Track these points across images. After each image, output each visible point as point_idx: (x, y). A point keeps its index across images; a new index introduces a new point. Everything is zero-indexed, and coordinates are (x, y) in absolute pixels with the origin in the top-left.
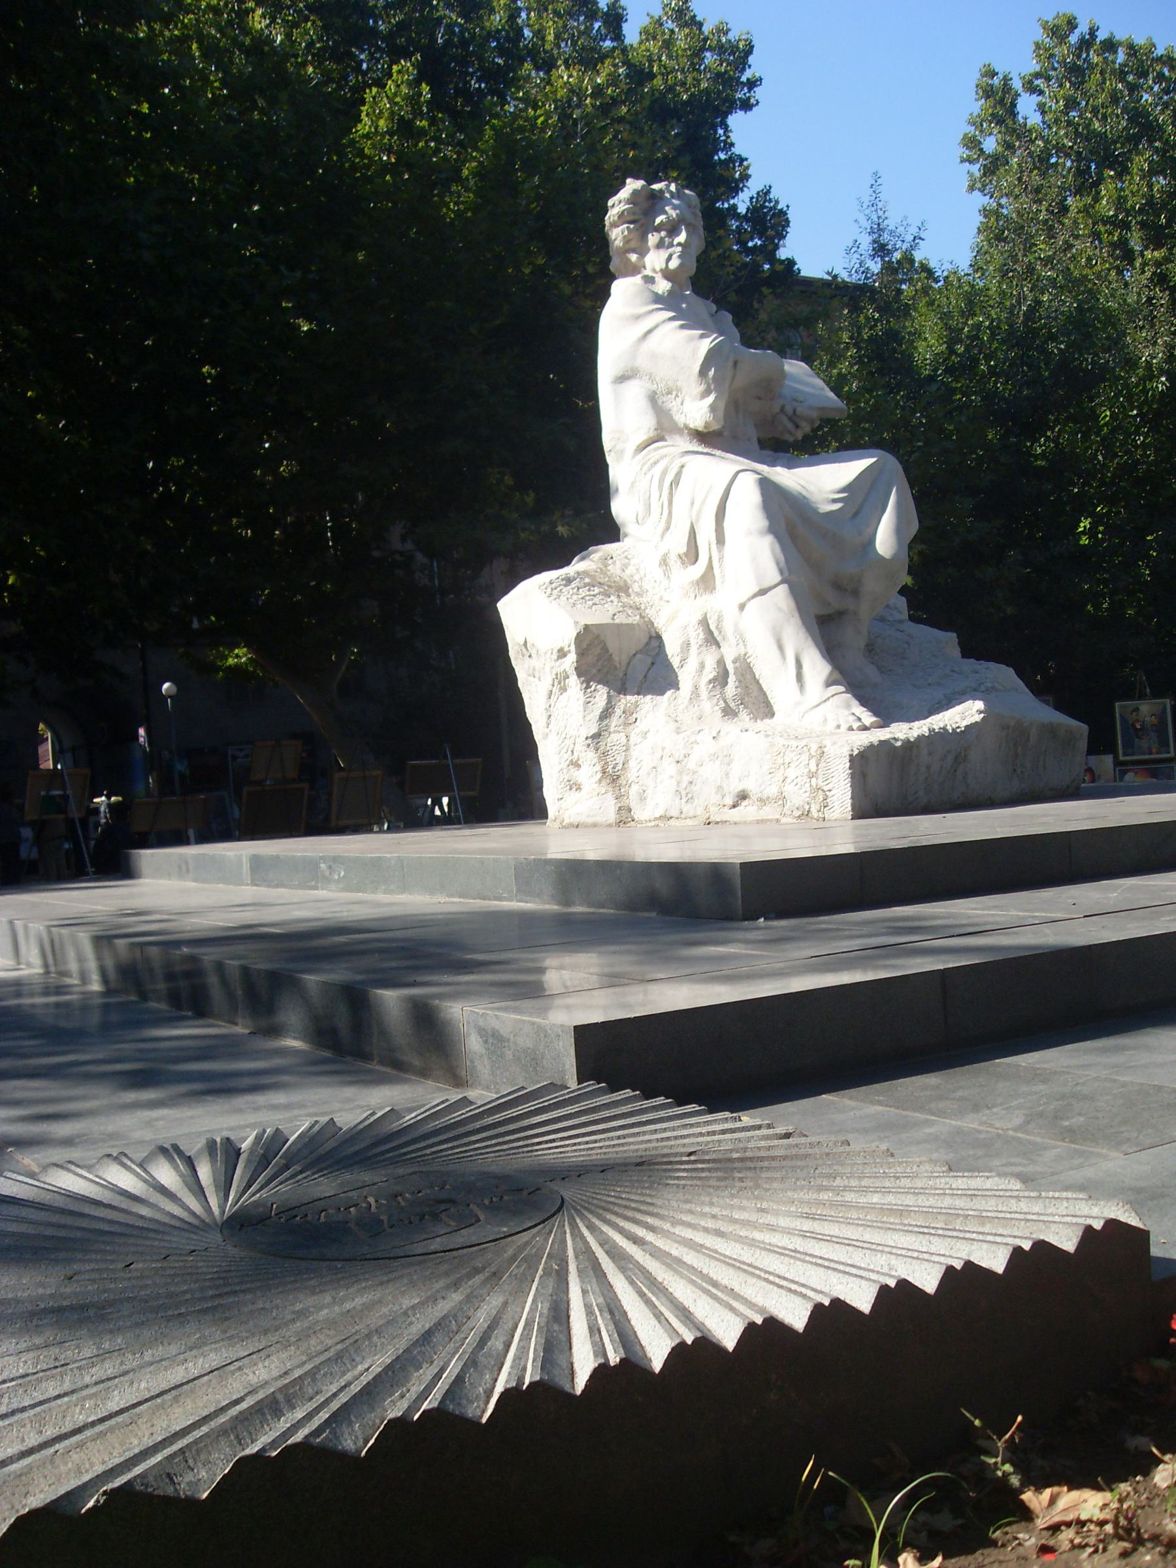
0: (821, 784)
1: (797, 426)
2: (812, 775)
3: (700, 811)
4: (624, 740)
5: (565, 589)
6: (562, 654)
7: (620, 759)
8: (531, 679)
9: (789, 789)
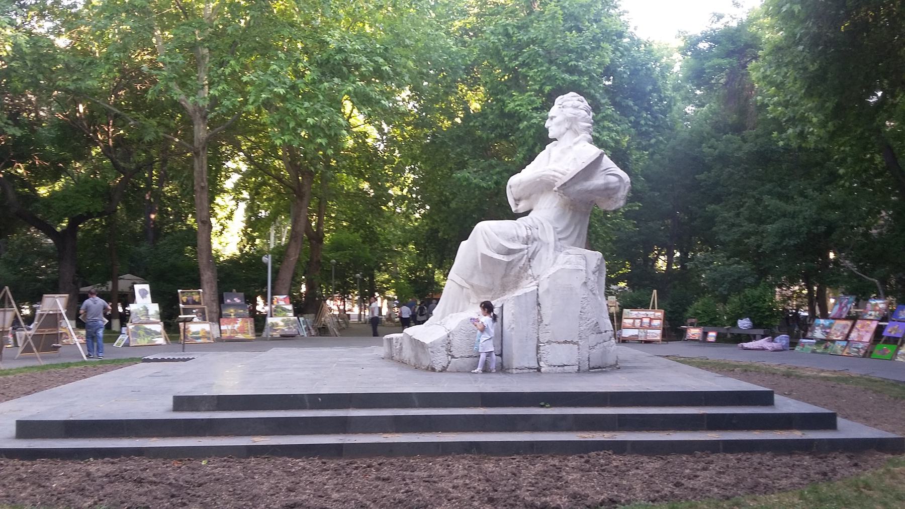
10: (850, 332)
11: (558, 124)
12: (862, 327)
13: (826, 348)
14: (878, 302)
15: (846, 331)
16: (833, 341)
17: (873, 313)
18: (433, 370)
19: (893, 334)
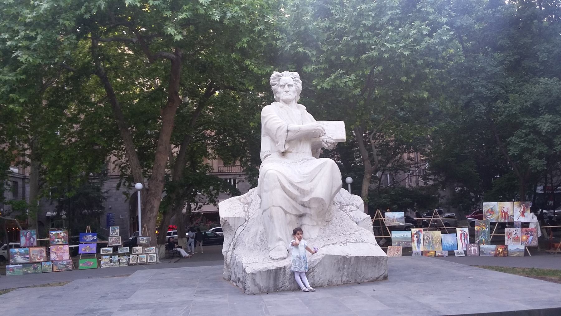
10: (48, 253)
11: (294, 92)
12: (58, 250)
13: (35, 268)
14: (58, 232)
15: (44, 254)
16: (40, 263)
17: (59, 240)
18: (385, 278)
19: (87, 251)
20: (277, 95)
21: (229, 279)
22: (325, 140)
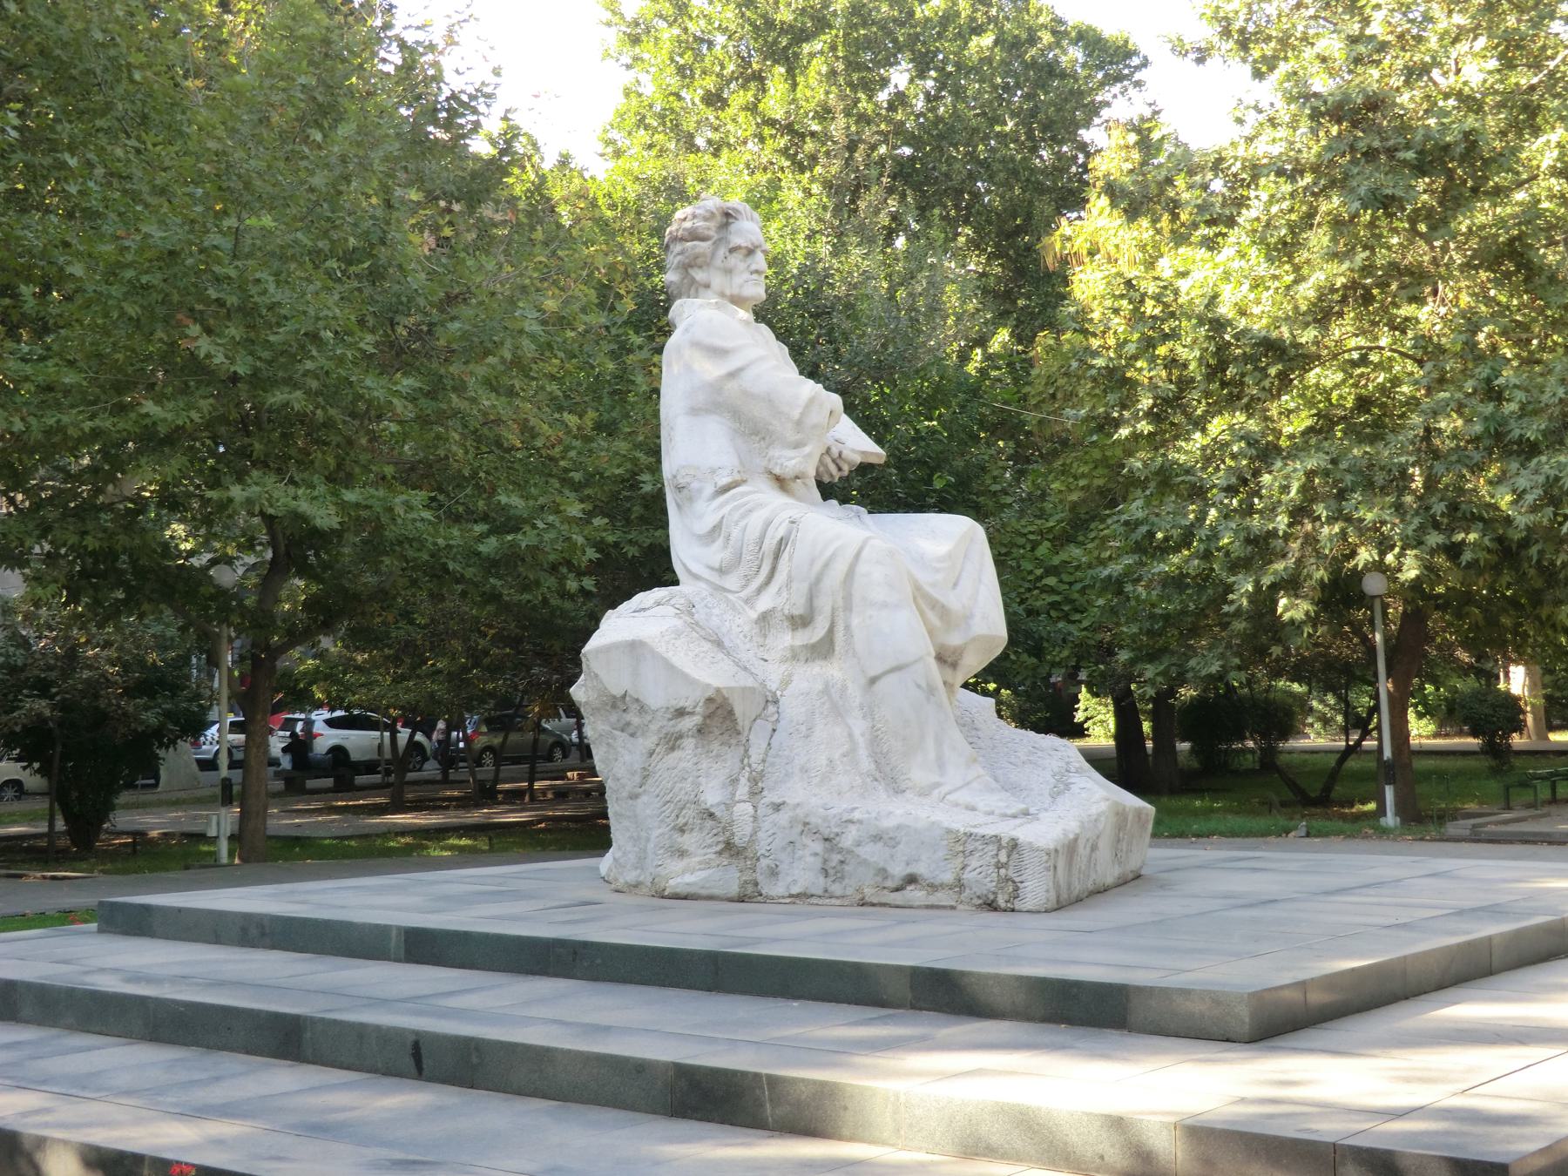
0: (1011, 873)
1: (840, 469)
2: (999, 865)
3: (849, 891)
4: (750, 810)
5: (678, 643)
6: (681, 713)
7: (748, 830)
8: (617, 733)
9: (968, 876)
20: (699, 275)
21: (747, 897)
22: (835, 452)
